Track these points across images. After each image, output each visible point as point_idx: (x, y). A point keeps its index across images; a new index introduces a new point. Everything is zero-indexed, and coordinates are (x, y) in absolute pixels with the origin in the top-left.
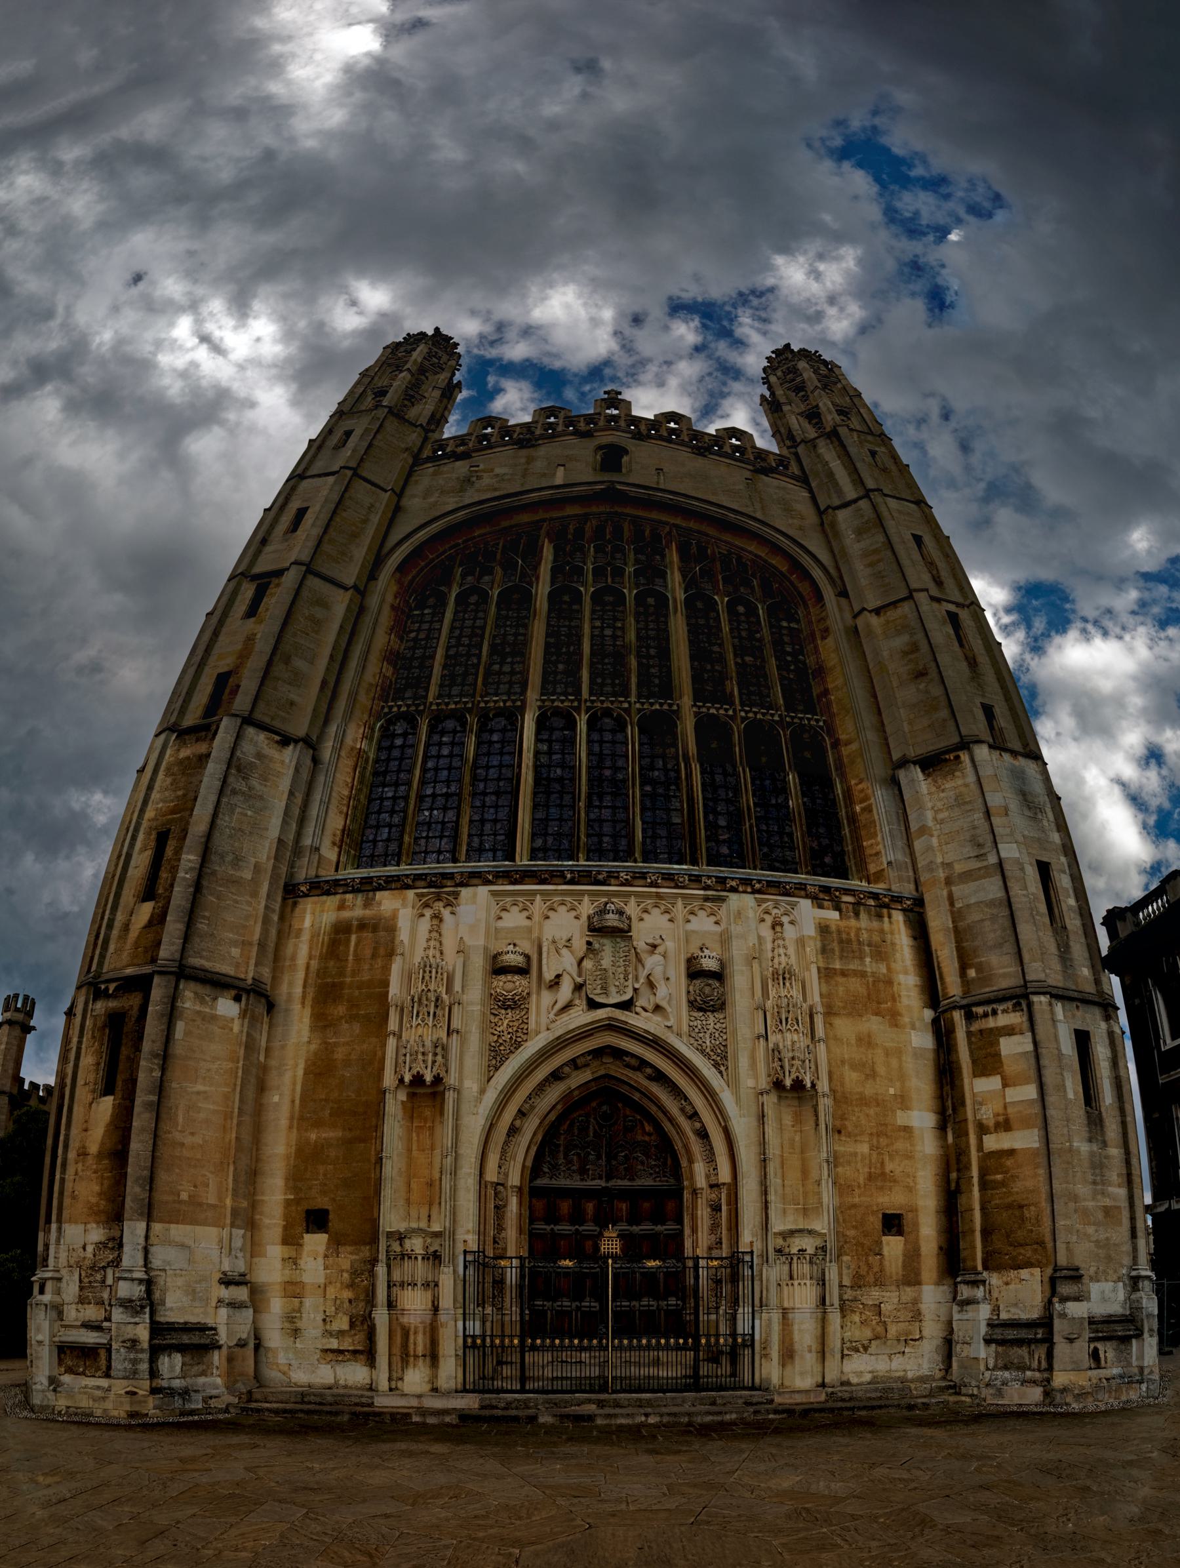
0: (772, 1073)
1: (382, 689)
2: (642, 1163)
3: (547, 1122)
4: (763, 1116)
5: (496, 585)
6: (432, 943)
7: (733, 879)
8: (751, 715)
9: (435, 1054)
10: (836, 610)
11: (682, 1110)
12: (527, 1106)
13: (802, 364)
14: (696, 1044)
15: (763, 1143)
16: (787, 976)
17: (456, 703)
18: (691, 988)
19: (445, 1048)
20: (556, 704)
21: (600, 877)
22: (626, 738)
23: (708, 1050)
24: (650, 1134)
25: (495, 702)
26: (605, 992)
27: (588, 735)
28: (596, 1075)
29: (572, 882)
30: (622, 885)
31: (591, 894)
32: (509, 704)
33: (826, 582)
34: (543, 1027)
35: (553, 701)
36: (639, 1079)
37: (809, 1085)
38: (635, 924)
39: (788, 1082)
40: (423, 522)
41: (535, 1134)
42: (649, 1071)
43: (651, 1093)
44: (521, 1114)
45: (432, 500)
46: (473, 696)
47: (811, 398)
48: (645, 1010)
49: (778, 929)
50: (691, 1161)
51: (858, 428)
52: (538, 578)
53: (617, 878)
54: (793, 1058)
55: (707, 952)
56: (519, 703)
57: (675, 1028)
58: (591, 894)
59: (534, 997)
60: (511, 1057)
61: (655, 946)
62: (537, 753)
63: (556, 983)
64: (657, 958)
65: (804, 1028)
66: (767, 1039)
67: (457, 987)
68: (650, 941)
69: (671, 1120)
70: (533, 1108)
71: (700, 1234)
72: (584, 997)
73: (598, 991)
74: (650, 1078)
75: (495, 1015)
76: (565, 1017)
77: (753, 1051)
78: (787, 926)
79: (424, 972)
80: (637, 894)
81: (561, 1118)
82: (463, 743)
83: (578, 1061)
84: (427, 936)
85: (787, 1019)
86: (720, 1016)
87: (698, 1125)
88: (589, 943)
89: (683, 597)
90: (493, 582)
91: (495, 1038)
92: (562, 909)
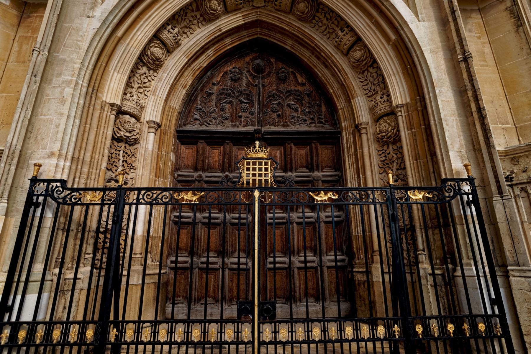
24: (303, 85)
50: (349, 99)
69: (326, 62)
71: (368, 173)
74: (302, 19)
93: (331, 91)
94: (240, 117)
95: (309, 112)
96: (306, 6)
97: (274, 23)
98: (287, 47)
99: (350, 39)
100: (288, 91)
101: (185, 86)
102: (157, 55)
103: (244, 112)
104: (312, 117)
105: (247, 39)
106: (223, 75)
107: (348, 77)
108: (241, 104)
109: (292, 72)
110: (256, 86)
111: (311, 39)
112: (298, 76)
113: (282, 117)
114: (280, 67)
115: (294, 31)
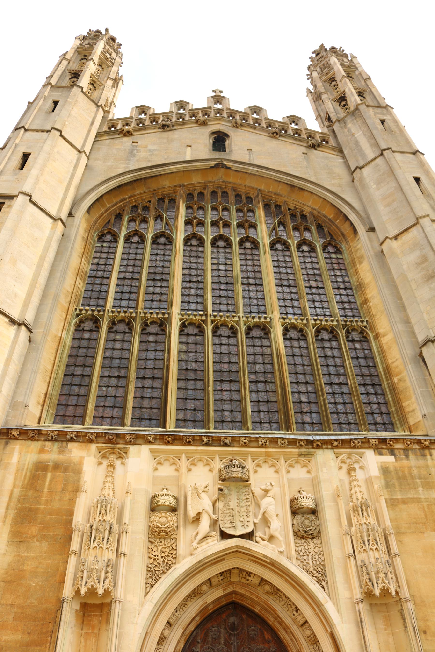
1: (76, 297)
5: (150, 231)
8: (318, 322)
10: (368, 242)
13: (334, 60)
14: (301, 565)
17: (125, 312)
20: (191, 317)
22: (237, 341)
23: (311, 569)
25: (151, 313)
27: (213, 340)
32: (160, 315)
33: (359, 222)
35: (189, 315)
37: (394, 593)
40: (104, 179)
42: (267, 588)
45: (109, 164)
46: (136, 308)
47: (340, 86)
51: (371, 104)
52: (177, 228)
56: (166, 316)
62: (180, 352)
65: (382, 547)
82: (130, 341)
89: (269, 242)
90: (147, 229)
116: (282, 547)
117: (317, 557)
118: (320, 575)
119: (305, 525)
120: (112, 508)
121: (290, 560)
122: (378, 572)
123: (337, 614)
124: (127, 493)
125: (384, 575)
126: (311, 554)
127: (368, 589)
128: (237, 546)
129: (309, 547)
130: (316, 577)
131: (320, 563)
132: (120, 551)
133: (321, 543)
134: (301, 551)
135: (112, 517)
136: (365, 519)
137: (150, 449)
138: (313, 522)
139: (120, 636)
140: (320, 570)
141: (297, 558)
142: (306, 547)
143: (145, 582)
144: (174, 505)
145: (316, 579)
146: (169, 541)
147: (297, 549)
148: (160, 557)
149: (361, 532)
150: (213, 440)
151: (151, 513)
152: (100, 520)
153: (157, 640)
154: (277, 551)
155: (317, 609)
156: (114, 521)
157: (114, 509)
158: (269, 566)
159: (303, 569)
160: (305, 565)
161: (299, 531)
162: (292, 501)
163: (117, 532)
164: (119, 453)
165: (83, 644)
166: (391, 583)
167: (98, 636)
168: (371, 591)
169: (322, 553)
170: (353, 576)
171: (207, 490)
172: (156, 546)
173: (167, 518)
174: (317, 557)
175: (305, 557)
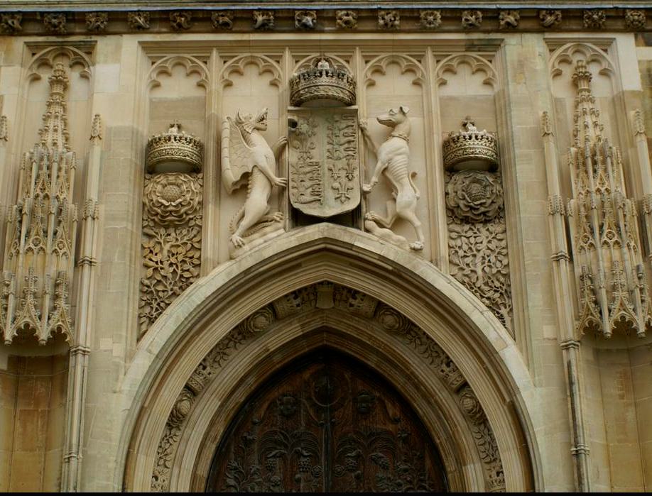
0: (582, 313)
2: (385, 468)
3: (231, 404)
4: (571, 384)
6: (51, 123)
7: (509, 11)
9: (56, 297)
11: (444, 380)
12: (199, 379)
14: (460, 274)
15: (572, 426)
16: (599, 158)
18: (450, 188)
19: (74, 289)
21: (308, 20)
24: (396, 421)
26: (318, 198)
28: (308, 329)
29: (264, 28)
30: (341, 30)
31: (293, 46)
34: (224, 253)
36: (377, 334)
38: (361, 91)
39: (608, 327)
41: (212, 424)
43: (394, 353)
44: (191, 391)
48: (381, 225)
49: (583, 85)
50: (461, 462)
53: (333, 19)
54: (614, 288)
55: (472, 130)
57: (426, 251)
58: (293, 46)
59: (210, 208)
60: (176, 301)
61: (392, 125)
63: (242, 187)
64: (396, 143)
66: (571, 260)
67: (93, 193)
68: (385, 117)
69: (428, 397)
70: (207, 382)
72: (286, 209)
73: (308, 198)
74: (391, 331)
75: (150, 237)
76: (257, 239)
77: (550, 279)
78: (596, 79)
79: (40, 168)
80: (363, 45)
81: (253, 397)
83: (279, 308)
84: (43, 110)
85: (601, 227)
86: (496, 228)
87: (468, 403)
88: (293, 124)
91: (150, 271)
92: (252, 72)
93: (438, 441)
94: (298, 481)
95: (405, 470)
96: (396, 320)
97: (349, 333)
98: (369, 363)
99: (458, 379)
100: (372, 434)
101: (216, 438)
102: (183, 411)
103: (303, 471)
104: (409, 479)
105: (307, 349)
106: (269, 406)
107: (458, 430)
108: (299, 458)
109: (379, 399)
110: (322, 425)
111: (405, 363)
112: (389, 405)
113: (362, 479)
114: (360, 388)
115: (380, 348)
116: (419, 240)
117: (493, 259)
118: (497, 295)
119: (470, 195)
120: (63, 171)
121: (437, 265)
122: (614, 288)
123: (526, 368)
124: (92, 138)
125: (627, 295)
126: (481, 254)
127: (591, 322)
128: (325, 240)
129: (479, 240)
130: (488, 298)
131: (499, 272)
132: (81, 257)
133: (505, 231)
134: (460, 247)
135: (64, 190)
136: (598, 181)
137: (139, 42)
138: (488, 188)
139: (87, 414)
140: (497, 284)
141: (451, 262)
142: (472, 240)
143: (137, 313)
144: (193, 159)
145: (487, 302)
146: (184, 232)
147: (453, 243)
148: (166, 264)
149: (589, 209)
150: (276, 18)
151: (148, 176)
152: (37, 196)
153: (165, 419)
154: (408, 248)
155: (485, 360)
156: (68, 196)
157: (66, 172)
158: (392, 277)
159: (463, 283)
160: (467, 276)
161: (458, 206)
162: (447, 145)
163: (76, 217)
164: (75, 54)
165: (19, 429)
166: (639, 310)
167: (47, 415)
168: (598, 325)
169: (504, 251)
170: (562, 296)
171: (263, 127)
172: (160, 243)
173: (178, 186)
174: (493, 259)
175: (468, 260)
